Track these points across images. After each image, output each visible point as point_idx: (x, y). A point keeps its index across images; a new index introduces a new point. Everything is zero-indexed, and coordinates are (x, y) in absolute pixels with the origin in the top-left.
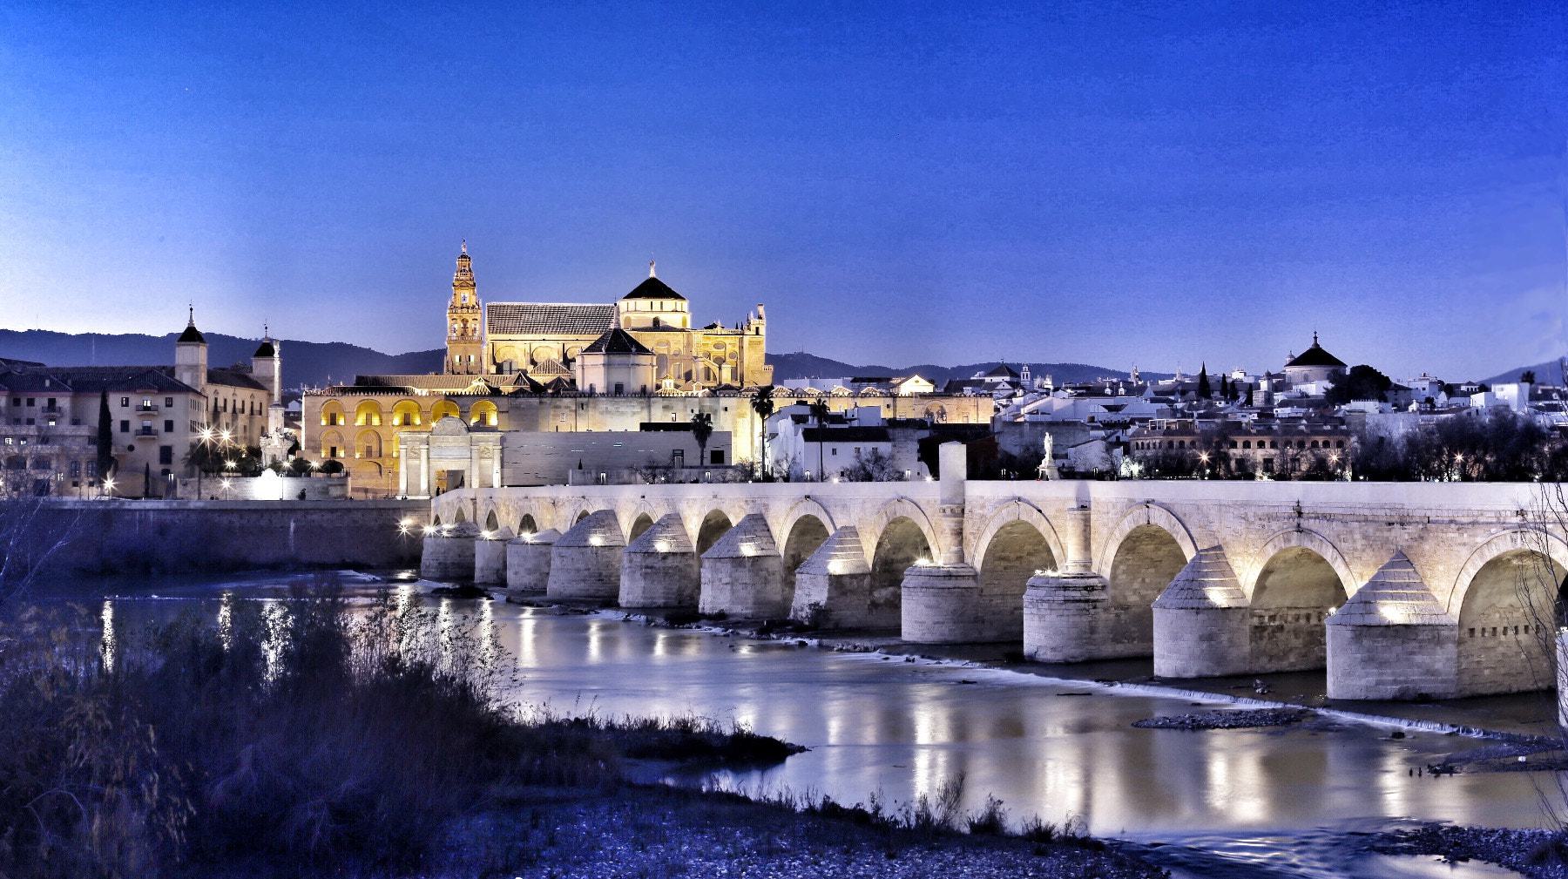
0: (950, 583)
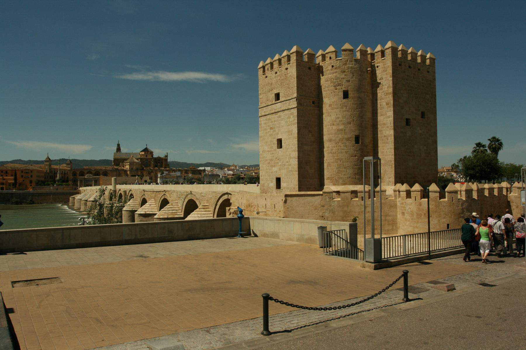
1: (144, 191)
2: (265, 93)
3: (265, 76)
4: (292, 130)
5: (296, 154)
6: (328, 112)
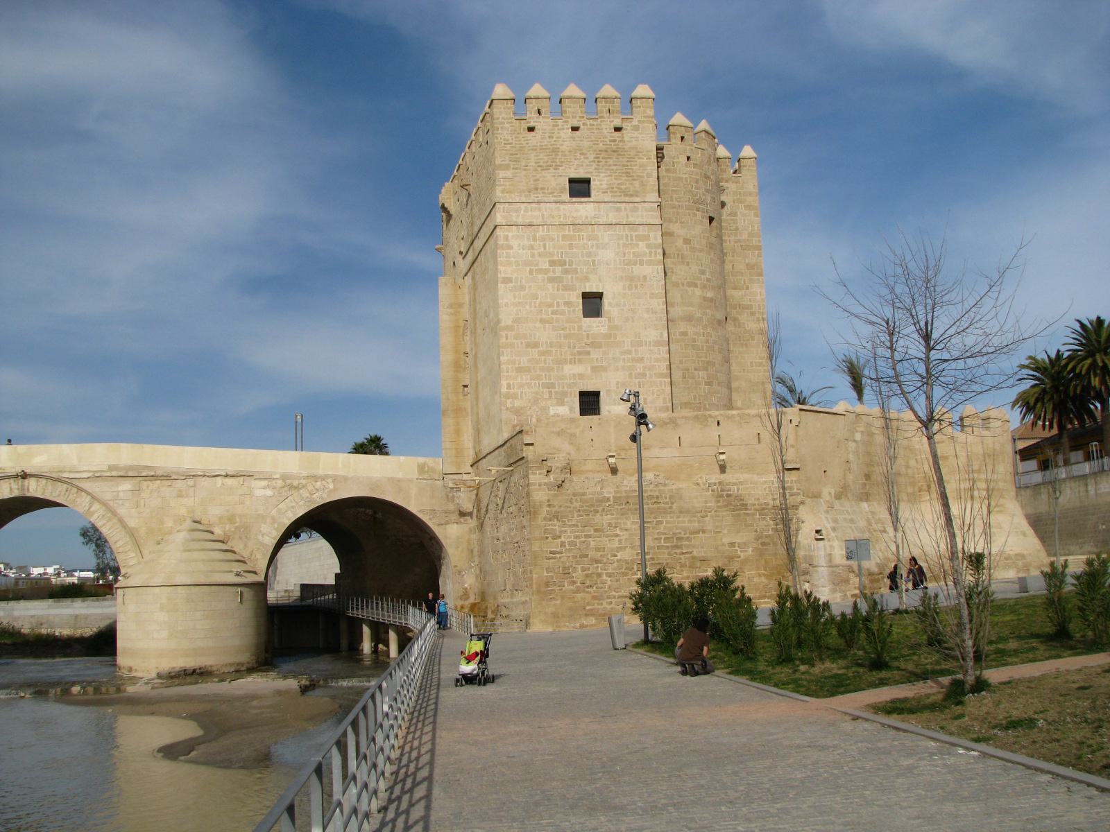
2: (525, 170)
3: (525, 125)
5: (661, 335)
6: (682, 254)
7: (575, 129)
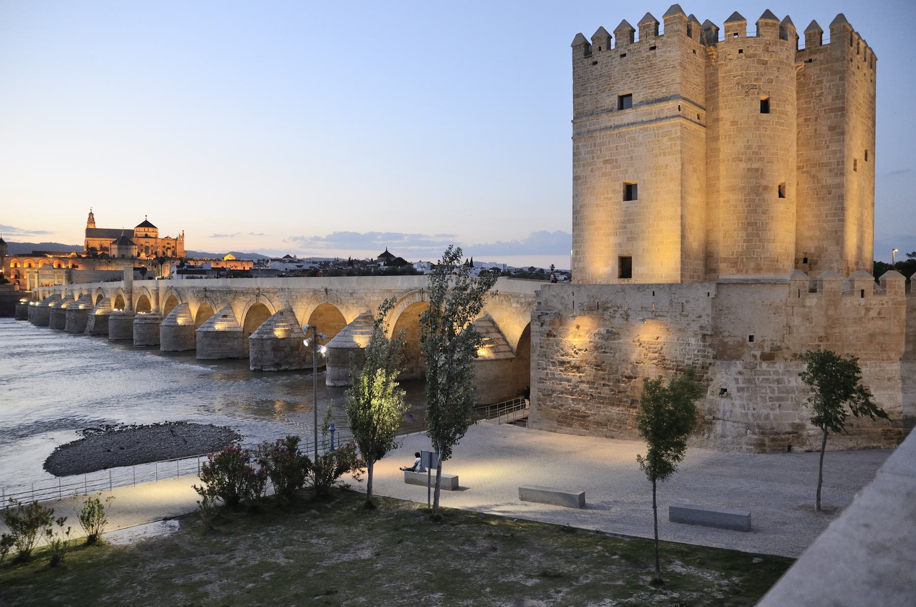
0: (123, 318)
1: (205, 290)
4: (667, 165)
5: (676, 212)
7: (624, 55)
